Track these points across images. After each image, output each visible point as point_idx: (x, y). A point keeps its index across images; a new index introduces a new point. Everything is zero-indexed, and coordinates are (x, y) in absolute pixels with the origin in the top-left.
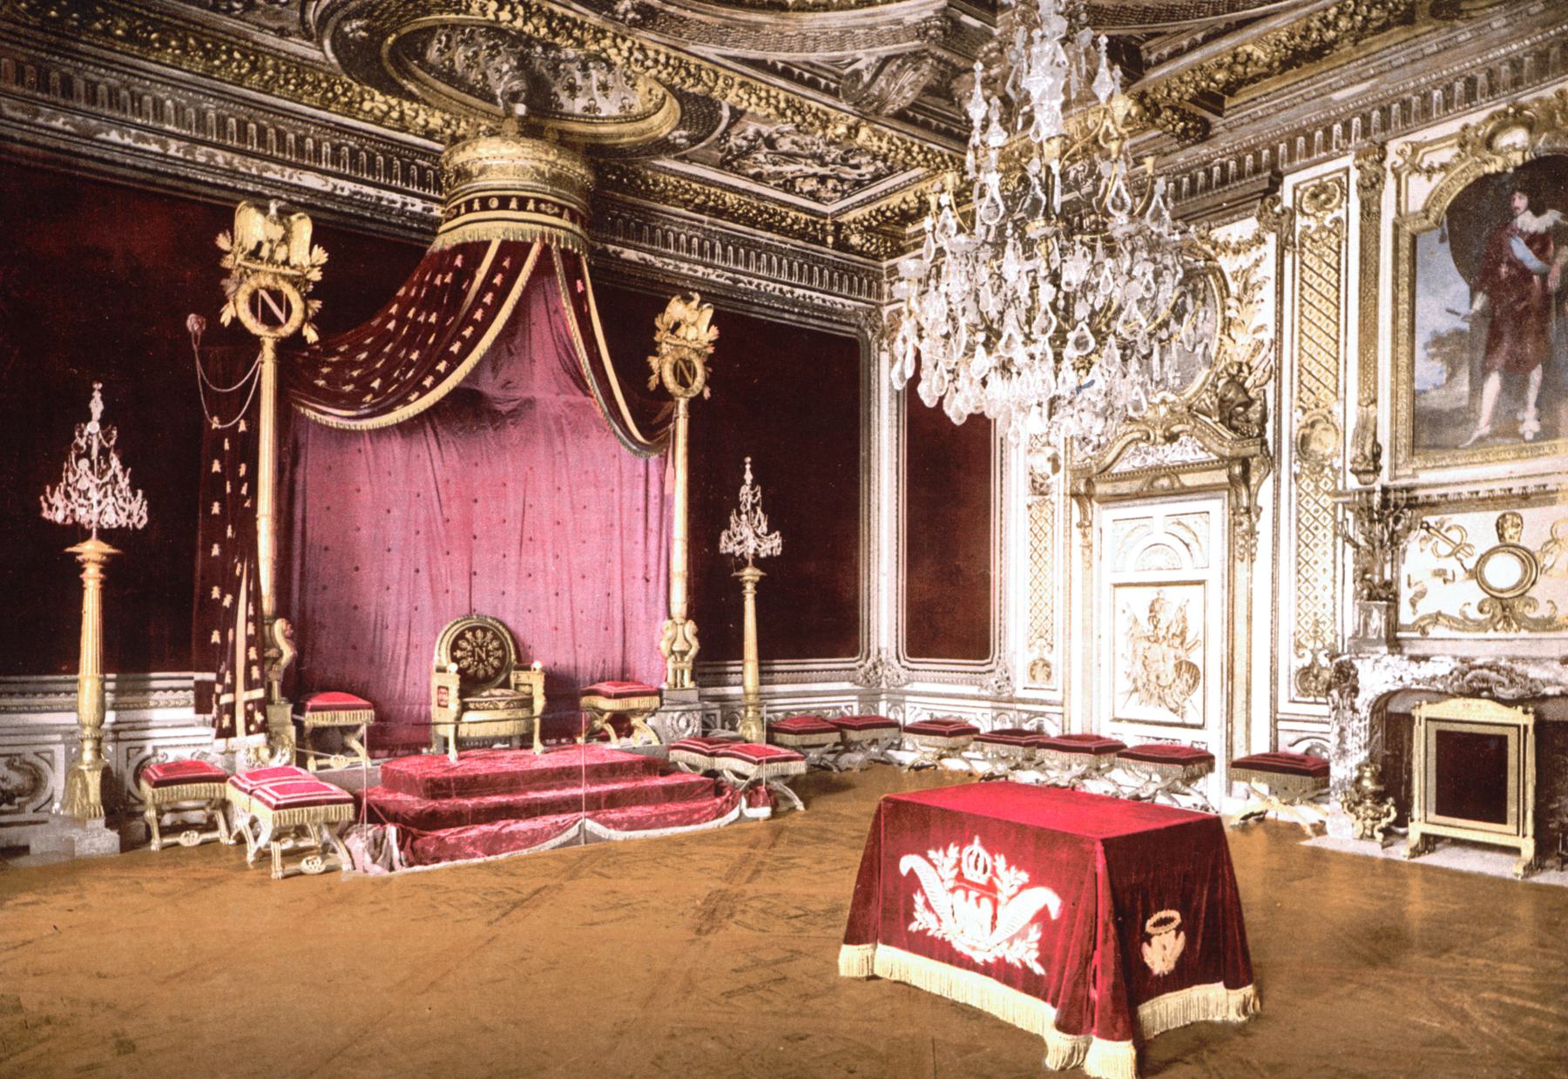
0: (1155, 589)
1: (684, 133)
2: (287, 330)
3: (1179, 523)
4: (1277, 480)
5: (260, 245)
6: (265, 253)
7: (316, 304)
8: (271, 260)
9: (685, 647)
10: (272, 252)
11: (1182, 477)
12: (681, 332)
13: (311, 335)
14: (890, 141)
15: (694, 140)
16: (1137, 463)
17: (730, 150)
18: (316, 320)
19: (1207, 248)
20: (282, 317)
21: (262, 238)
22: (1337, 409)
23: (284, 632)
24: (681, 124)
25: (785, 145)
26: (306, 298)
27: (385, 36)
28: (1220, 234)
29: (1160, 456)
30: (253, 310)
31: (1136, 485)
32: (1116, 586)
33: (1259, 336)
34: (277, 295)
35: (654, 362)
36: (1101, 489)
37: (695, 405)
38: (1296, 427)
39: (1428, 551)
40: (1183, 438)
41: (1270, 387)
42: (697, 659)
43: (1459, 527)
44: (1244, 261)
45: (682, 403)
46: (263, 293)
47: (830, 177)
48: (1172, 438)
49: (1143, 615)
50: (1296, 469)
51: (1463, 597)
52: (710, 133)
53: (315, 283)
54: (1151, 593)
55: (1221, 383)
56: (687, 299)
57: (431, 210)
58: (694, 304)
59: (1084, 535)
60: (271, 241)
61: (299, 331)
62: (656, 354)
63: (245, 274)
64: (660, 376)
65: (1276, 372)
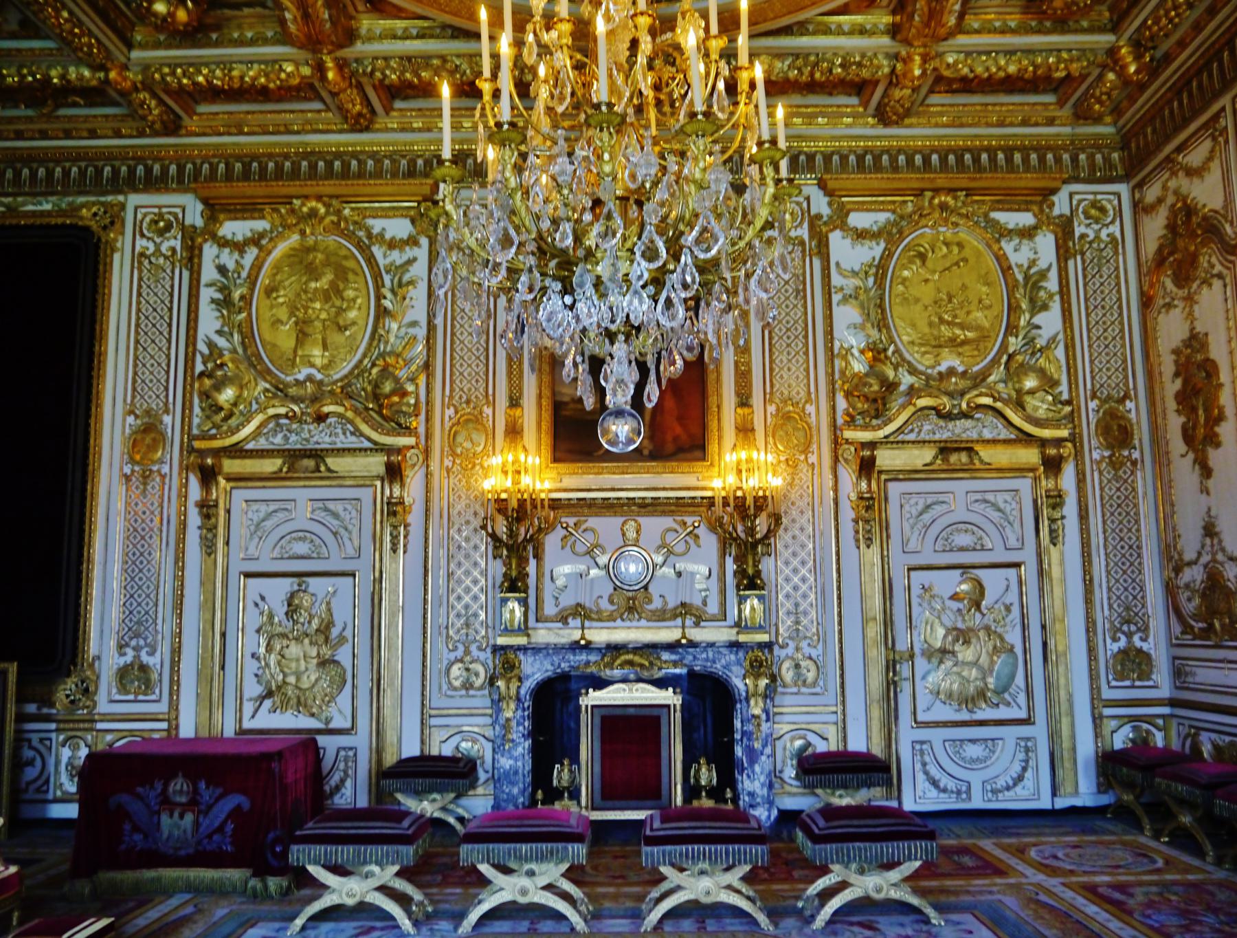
0: (295, 580)
3: (326, 509)
4: (428, 475)
11: (329, 461)
16: (278, 440)
19: (361, 234)
22: (488, 411)
28: (377, 225)
29: (305, 435)
31: (270, 465)
32: (248, 575)
33: (412, 331)
36: (231, 466)
38: (447, 425)
39: (568, 548)
40: (331, 420)
41: (422, 380)
43: (593, 530)
44: (397, 257)
48: (321, 418)
49: (280, 610)
50: (447, 463)
51: (599, 592)
54: (287, 585)
55: (375, 371)
59: (207, 517)
65: (427, 366)
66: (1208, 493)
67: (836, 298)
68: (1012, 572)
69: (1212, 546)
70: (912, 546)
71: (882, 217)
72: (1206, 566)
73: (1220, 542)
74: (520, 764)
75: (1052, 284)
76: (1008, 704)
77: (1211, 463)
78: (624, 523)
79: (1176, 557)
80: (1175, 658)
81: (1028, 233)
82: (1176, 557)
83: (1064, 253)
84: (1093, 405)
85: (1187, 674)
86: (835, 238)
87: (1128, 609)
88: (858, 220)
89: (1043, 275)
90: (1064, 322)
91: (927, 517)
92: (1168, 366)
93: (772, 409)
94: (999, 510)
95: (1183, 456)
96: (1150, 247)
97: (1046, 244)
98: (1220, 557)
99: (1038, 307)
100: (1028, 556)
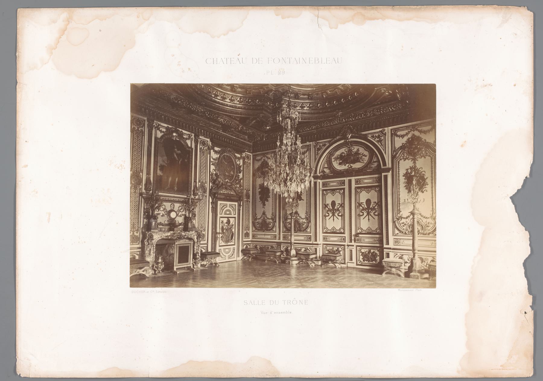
43: (165, 205)
66: (264, 208)
67: (211, 163)
68: (234, 219)
69: (264, 216)
70: (221, 213)
71: (219, 149)
72: (262, 220)
73: (266, 216)
74: (152, 260)
75: (242, 169)
76: (232, 242)
77: (266, 204)
78: (171, 205)
79: (255, 217)
80: (253, 234)
81: (239, 159)
82: (255, 217)
83: (244, 163)
84: (245, 191)
85: (255, 236)
86: (212, 151)
87: (247, 226)
88: (216, 149)
89: (241, 166)
90: (243, 176)
91: (223, 208)
92: (258, 187)
93: (200, 183)
94: (233, 208)
95: (259, 202)
96: (256, 166)
97: (241, 161)
98: (266, 218)
99: (240, 173)
100: (236, 216)
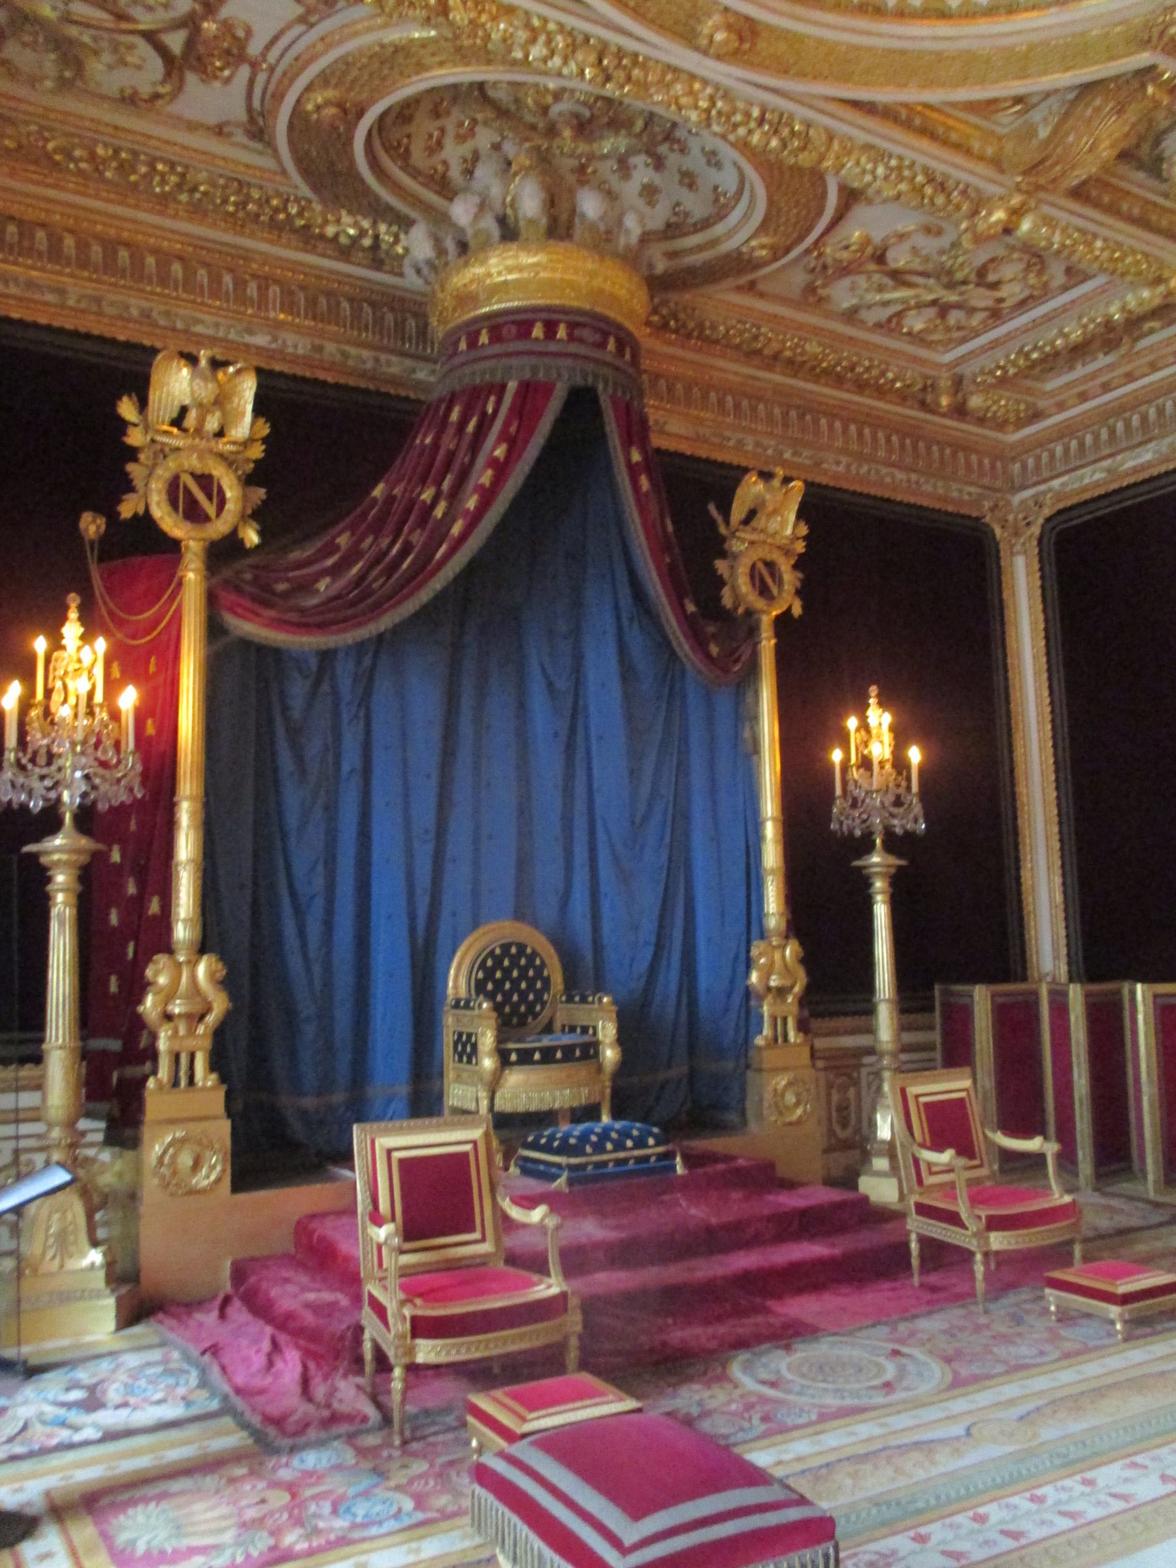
1: (765, 240)
2: (219, 528)
5: (184, 410)
6: (191, 420)
7: (260, 493)
8: (199, 431)
9: (788, 983)
10: (201, 421)
12: (760, 522)
13: (252, 537)
14: (1064, 230)
15: (778, 252)
17: (825, 267)
18: (258, 515)
20: (211, 510)
21: (187, 402)
23: (211, 975)
24: (763, 227)
25: (899, 258)
26: (249, 481)
27: (361, 113)
30: (173, 502)
34: (205, 481)
35: (721, 566)
37: (783, 622)
42: (803, 1001)
45: (766, 623)
46: (187, 479)
47: (958, 306)
52: (801, 239)
53: (256, 462)
56: (766, 476)
57: (414, 371)
58: (776, 483)
60: (200, 406)
61: (234, 532)
62: (723, 554)
63: (163, 453)
64: (734, 589)
